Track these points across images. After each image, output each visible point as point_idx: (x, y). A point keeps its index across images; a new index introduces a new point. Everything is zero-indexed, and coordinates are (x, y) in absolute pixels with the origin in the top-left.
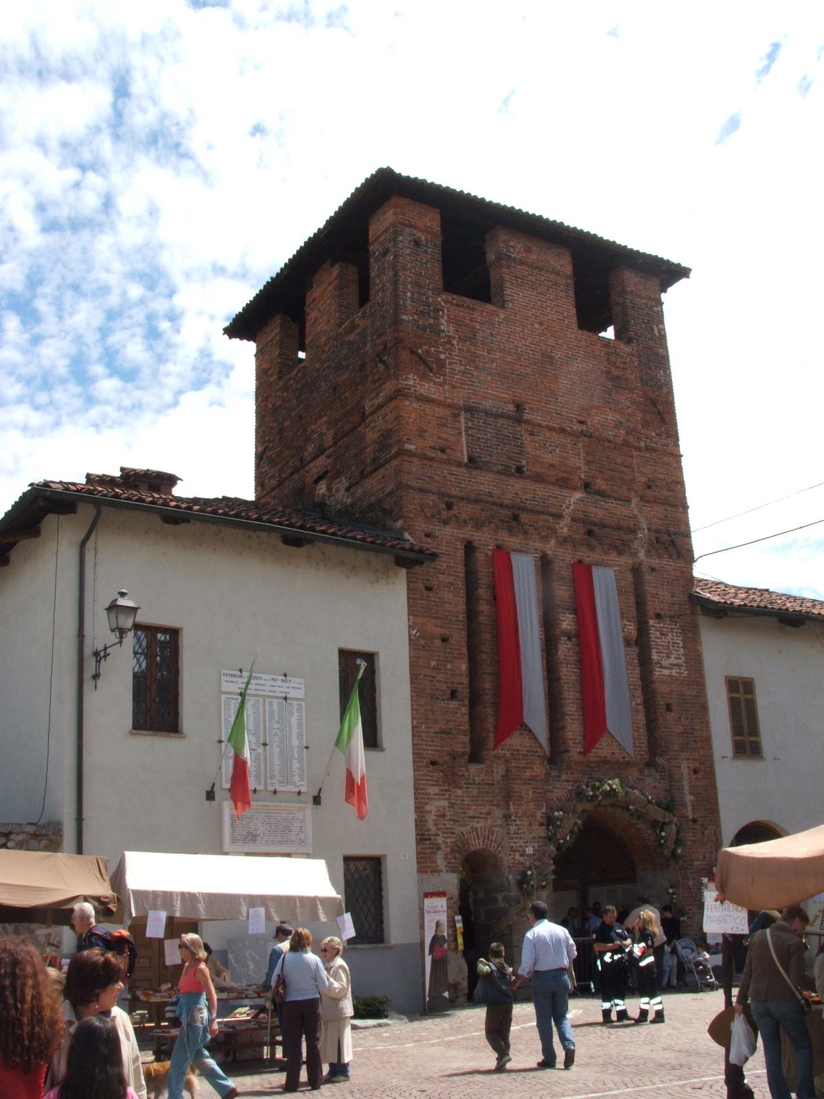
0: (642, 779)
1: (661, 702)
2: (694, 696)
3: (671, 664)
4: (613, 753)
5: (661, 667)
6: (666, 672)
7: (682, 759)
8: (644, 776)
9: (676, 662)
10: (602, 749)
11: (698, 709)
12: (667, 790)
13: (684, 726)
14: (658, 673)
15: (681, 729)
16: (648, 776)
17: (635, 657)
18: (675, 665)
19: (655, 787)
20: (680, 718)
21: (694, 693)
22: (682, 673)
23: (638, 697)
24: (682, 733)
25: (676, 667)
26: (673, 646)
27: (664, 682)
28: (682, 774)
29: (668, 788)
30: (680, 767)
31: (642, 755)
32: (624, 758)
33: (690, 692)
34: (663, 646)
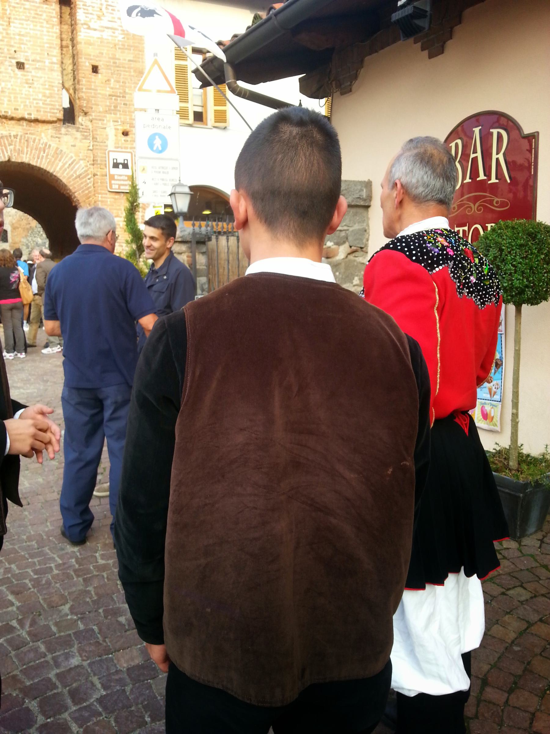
0: (59, 138)
1: (85, 66)
2: (130, 61)
3: (102, 27)
4: (16, 109)
5: (89, 28)
6: (96, 34)
7: (109, 121)
8: (61, 134)
9: (110, 25)
10: (3, 104)
11: (132, 74)
12: (91, 150)
13: (112, 88)
14: (82, 35)
15: (108, 91)
16: (66, 134)
17: (54, 15)
18: (108, 28)
19: (74, 146)
20: (109, 80)
21: (131, 57)
22: (116, 37)
23: (55, 56)
24: (110, 95)
25: (110, 31)
26: (107, 8)
27: (90, 44)
28: (107, 135)
29: (91, 148)
30: (105, 128)
31: (53, 113)
32: (30, 114)
33: (125, 57)
34: (93, 7)
